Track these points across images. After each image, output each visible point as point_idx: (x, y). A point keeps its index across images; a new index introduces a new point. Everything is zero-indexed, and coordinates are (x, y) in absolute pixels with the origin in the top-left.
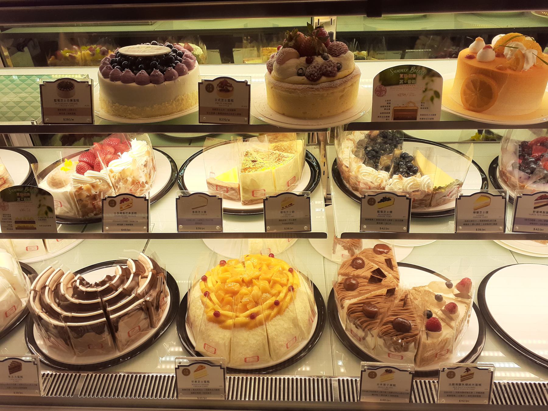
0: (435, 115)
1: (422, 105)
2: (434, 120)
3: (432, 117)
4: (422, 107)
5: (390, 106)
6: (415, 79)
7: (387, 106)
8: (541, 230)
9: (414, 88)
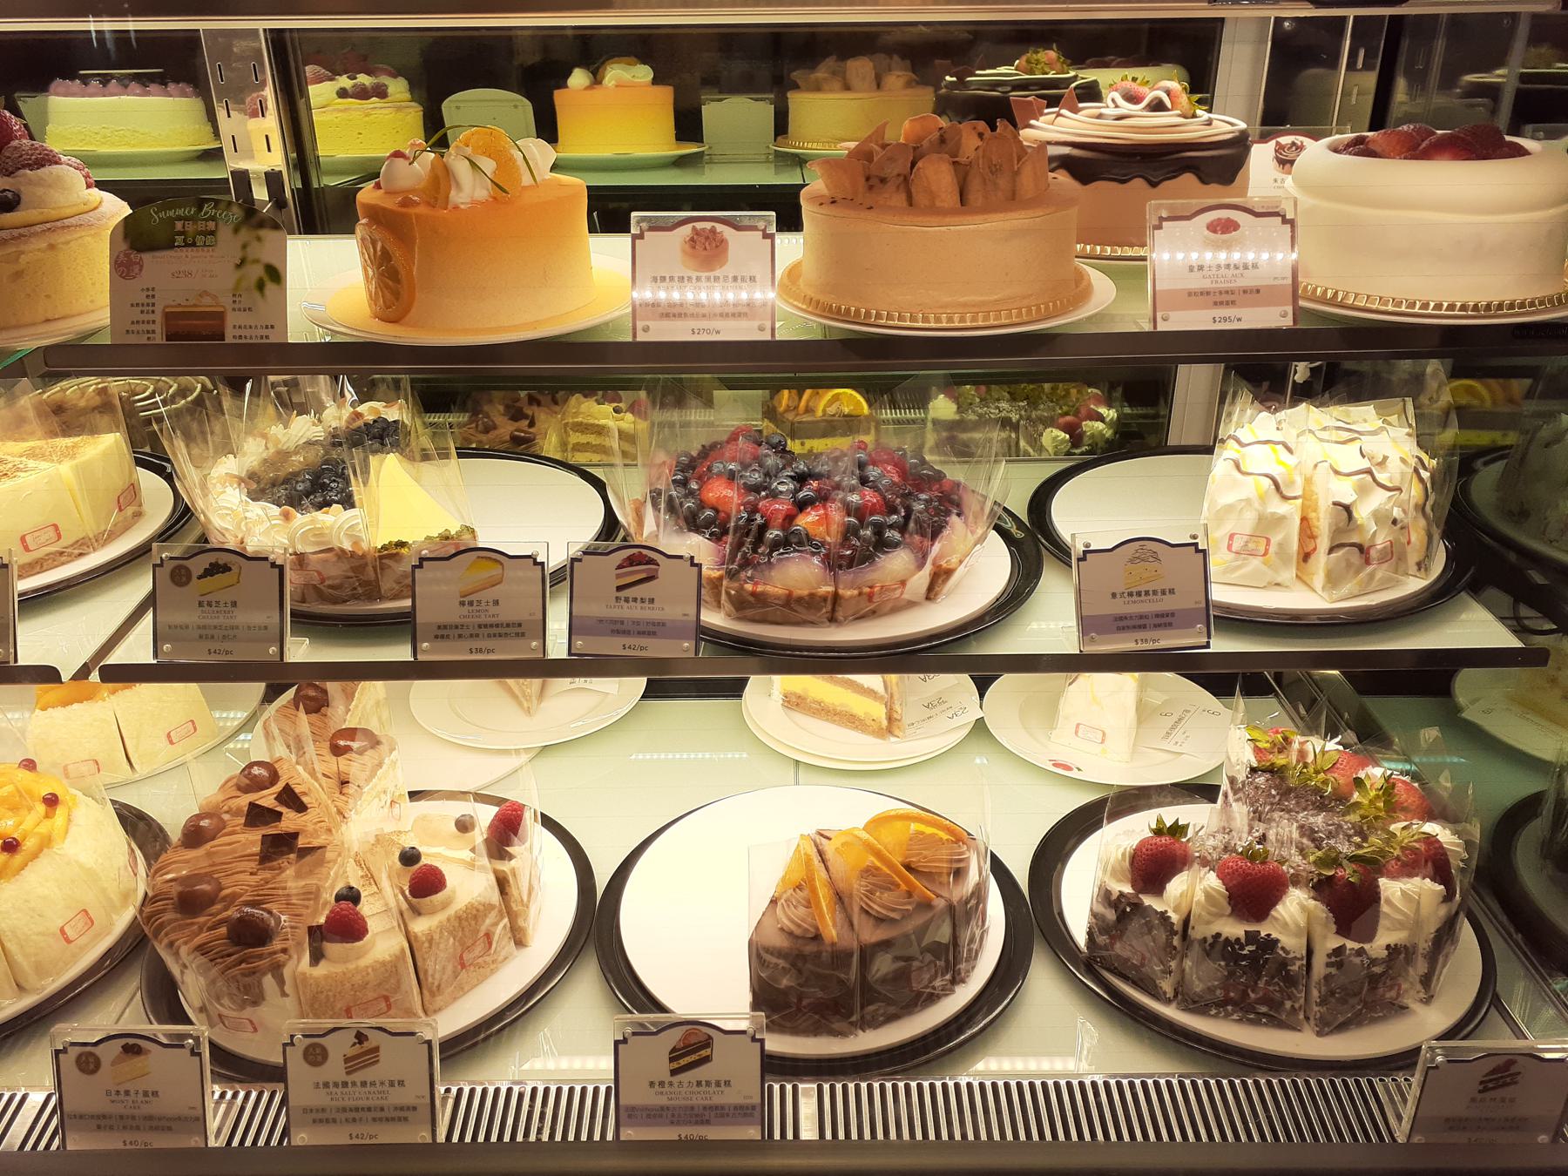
0: (272, 327)
1: (234, 302)
2: (273, 340)
3: (265, 332)
4: (236, 306)
5: (153, 305)
6: (212, 233)
7: (148, 305)
8: (642, 648)
9: (211, 256)
